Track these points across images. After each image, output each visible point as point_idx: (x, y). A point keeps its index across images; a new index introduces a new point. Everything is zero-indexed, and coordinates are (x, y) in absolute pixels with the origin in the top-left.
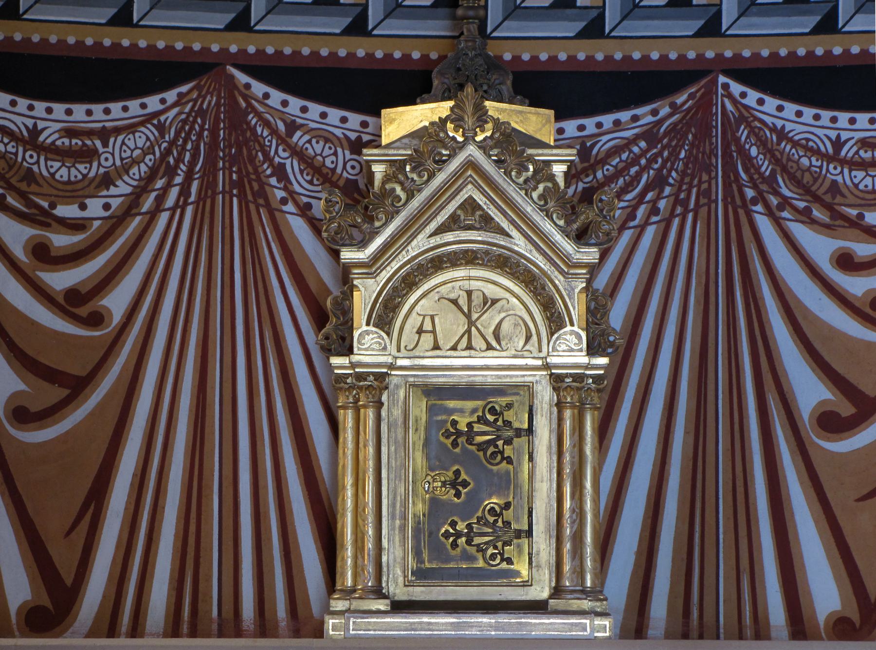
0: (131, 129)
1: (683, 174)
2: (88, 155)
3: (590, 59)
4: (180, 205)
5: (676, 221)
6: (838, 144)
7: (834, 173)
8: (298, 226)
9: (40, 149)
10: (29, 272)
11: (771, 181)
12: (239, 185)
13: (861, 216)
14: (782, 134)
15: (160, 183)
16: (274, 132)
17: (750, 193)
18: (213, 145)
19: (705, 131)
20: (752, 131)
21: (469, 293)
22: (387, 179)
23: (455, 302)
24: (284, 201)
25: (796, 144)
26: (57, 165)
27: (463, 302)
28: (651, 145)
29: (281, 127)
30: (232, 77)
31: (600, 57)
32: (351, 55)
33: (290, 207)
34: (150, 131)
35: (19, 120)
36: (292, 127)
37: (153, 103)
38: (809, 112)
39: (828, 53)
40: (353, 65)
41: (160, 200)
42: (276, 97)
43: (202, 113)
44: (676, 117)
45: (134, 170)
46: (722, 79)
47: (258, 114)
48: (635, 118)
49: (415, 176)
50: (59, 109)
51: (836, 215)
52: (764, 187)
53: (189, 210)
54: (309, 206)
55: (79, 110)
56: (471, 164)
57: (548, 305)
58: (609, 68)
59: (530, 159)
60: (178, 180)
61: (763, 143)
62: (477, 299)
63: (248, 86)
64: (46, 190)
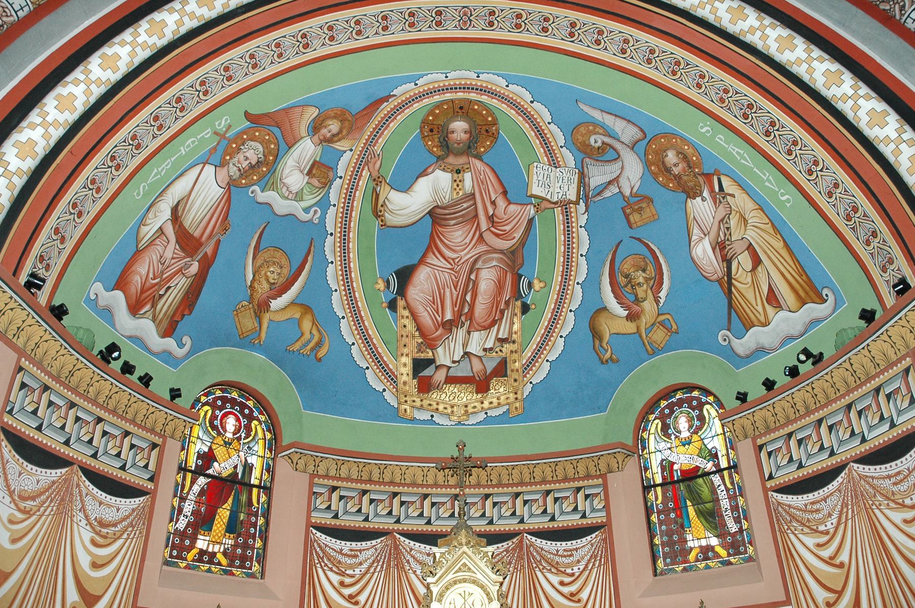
0: (368, 549)
1: (516, 561)
2: (356, 556)
3: (490, 530)
4: (381, 571)
5: (515, 574)
6: (558, 551)
7: (557, 559)
8: (413, 576)
9: (343, 554)
10: (338, 589)
11: (540, 561)
12: (397, 565)
13: (565, 570)
14: (542, 549)
15: (375, 565)
16: (406, 551)
17: (534, 565)
18: (390, 554)
19: (521, 549)
20: (534, 548)
21: (464, 592)
22: (440, 557)
23: (460, 594)
24: (409, 570)
25: (546, 551)
26: (347, 559)
27: (463, 595)
28: (507, 553)
29: (409, 550)
30: (395, 536)
31: (493, 530)
32: (427, 530)
33: (411, 571)
34: (373, 550)
35: (337, 546)
36: (411, 549)
37: (374, 542)
38: (549, 543)
39: (553, 527)
40: (427, 533)
41: (375, 569)
42: (407, 541)
43: (387, 545)
44: (514, 545)
45: (368, 561)
46: (525, 535)
47: (402, 546)
48: (503, 546)
49: (448, 556)
50: (348, 543)
51: (559, 570)
52: (538, 563)
53: (383, 572)
54: (416, 571)
55: (354, 544)
56: (464, 553)
57: (488, 594)
58: (495, 533)
59: (482, 551)
60: (380, 564)
61: (537, 552)
62: (467, 593)
63: (399, 538)
64: (344, 566)
